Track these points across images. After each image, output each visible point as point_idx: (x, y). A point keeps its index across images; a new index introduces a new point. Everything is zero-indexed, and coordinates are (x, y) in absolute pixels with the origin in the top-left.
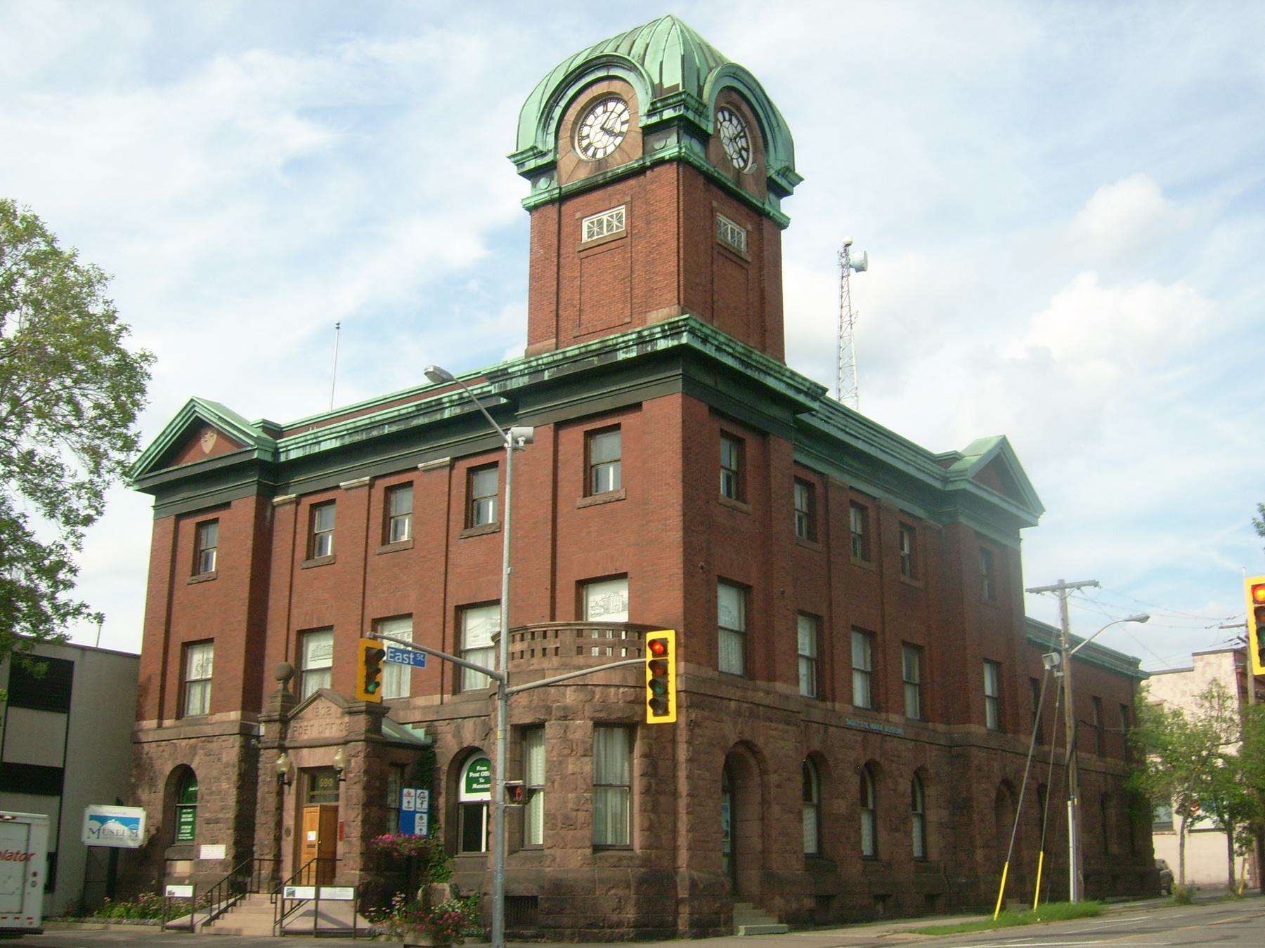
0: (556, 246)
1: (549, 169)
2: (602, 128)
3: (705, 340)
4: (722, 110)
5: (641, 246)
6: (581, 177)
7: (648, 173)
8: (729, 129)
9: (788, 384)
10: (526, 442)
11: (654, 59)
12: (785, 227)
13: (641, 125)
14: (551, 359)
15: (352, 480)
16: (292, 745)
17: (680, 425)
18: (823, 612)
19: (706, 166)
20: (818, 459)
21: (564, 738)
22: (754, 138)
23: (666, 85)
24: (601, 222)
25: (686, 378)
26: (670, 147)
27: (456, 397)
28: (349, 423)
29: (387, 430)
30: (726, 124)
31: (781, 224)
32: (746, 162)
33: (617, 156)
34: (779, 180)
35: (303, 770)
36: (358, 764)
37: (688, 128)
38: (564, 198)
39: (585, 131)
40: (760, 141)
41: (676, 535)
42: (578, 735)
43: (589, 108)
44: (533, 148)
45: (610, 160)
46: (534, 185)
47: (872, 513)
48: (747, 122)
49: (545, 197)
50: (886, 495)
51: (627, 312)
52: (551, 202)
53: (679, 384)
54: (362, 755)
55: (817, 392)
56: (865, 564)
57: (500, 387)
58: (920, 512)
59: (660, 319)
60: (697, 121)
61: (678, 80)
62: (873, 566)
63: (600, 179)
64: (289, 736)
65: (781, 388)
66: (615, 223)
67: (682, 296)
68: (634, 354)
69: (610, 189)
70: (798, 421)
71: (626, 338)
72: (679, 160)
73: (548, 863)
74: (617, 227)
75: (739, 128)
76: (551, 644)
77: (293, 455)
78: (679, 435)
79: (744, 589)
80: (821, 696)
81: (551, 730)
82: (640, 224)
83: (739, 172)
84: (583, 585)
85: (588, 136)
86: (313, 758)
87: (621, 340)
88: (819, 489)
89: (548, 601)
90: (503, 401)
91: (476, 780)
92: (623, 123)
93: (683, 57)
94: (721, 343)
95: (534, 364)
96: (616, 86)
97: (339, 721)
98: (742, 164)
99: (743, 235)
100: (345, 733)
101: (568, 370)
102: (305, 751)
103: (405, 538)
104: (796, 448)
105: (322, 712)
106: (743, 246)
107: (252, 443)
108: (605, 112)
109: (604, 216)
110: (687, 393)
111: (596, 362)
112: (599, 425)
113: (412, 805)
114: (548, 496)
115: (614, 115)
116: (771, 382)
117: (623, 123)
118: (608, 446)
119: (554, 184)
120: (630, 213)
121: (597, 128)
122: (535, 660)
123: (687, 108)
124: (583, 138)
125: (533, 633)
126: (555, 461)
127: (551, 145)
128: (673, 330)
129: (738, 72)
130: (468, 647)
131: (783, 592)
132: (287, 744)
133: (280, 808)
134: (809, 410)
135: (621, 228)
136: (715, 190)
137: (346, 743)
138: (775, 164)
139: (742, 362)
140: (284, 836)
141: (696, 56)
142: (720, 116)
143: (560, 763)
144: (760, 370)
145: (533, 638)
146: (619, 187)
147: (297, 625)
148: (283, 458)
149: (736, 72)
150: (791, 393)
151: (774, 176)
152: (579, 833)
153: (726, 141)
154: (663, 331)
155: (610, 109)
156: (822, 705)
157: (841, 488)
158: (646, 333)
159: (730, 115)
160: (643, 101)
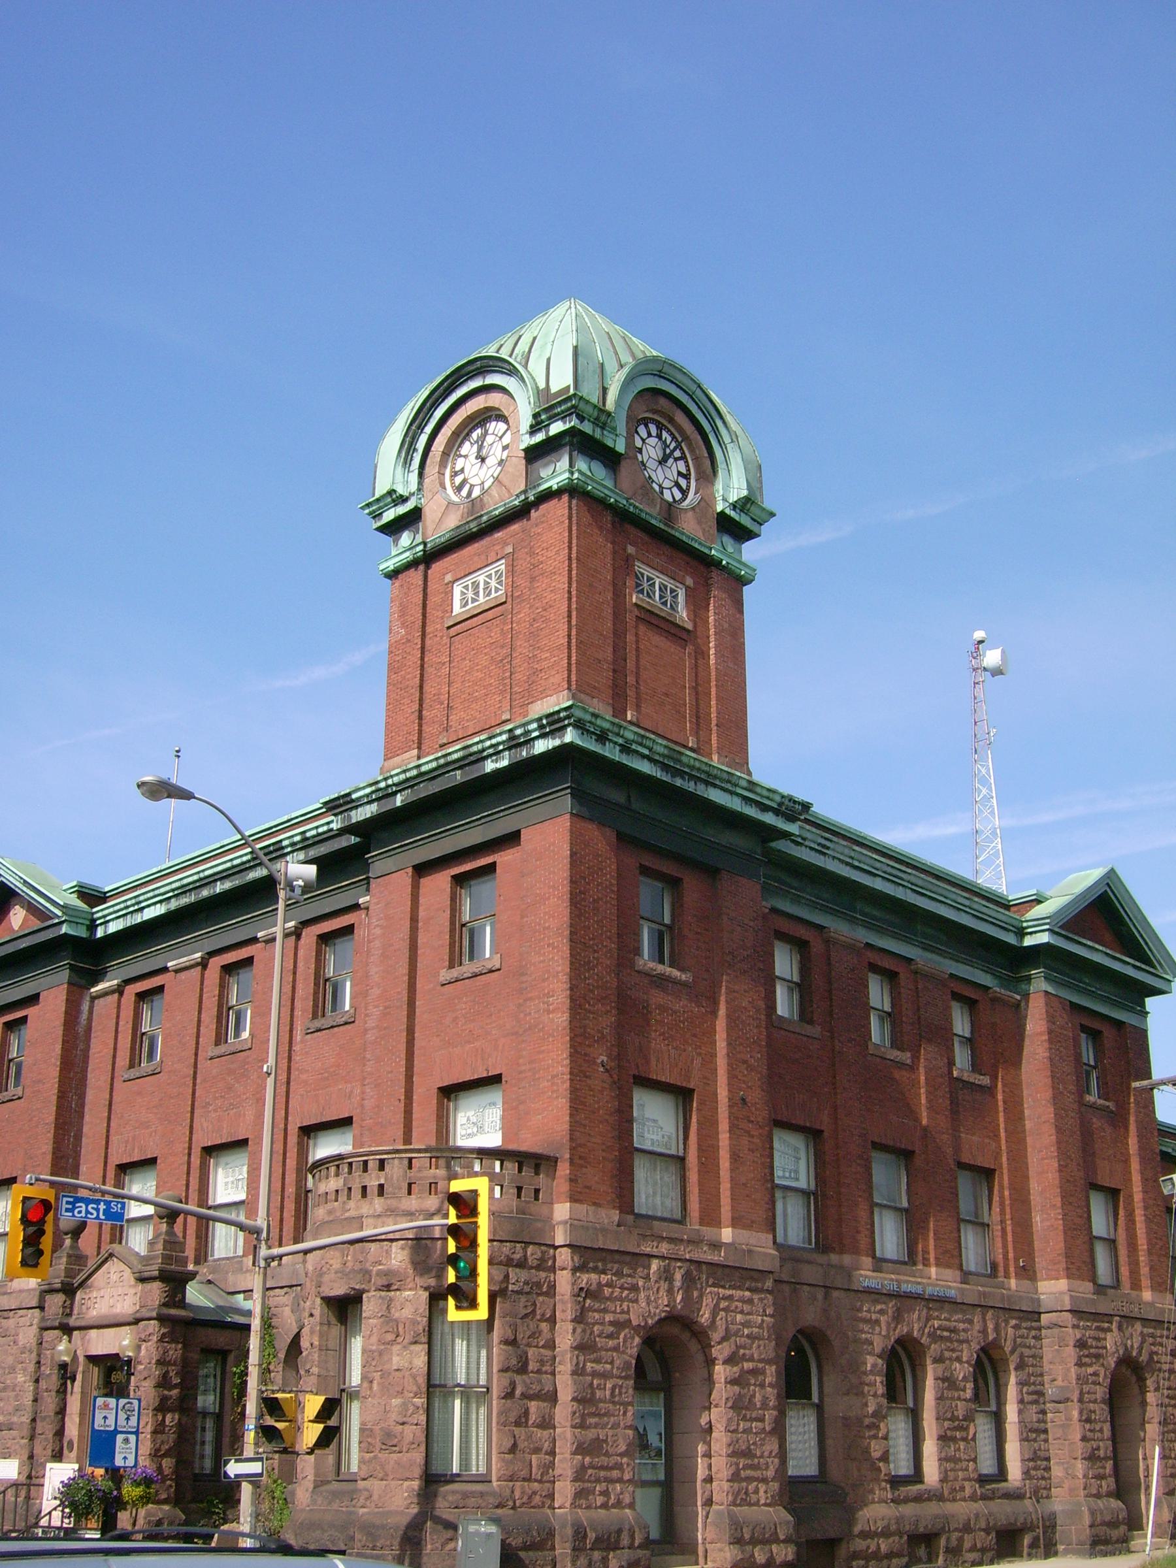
1: (413, 518)
3: (602, 738)
4: (645, 422)
5: (523, 614)
6: (452, 522)
9: (745, 798)
11: (540, 356)
12: (750, 582)
13: (523, 446)
14: (402, 777)
15: (181, 956)
16: (78, 1324)
17: (567, 861)
18: (824, 1122)
20: (814, 906)
21: (387, 1318)
22: (696, 459)
23: (554, 388)
24: (472, 588)
25: (578, 795)
26: (558, 472)
27: (298, 838)
28: (175, 882)
29: (219, 888)
32: (684, 493)
33: (494, 493)
35: (93, 1359)
36: (148, 1353)
37: (583, 444)
38: (430, 557)
39: (460, 463)
41: (562, 1019)
42: (406, 1313)
44: (391, 492)
45: (486, 498)
48: (686, 438)
50: (929, 955)
51: (506, 705)
53: (567, 801)
54: (155, 1338)
55: (796, 810)
57: (343, 820)
58: (985, 979)
60: (598, 435)
61: (568, 380)
64: (75, 1312)
65: (735, 804)
66: (493, 583)
67: (574, 678)
68: (504, 763)
70: (768, 852)
71: (494, 741)
72: (571, 490)
73: (362, 1501)
74: (497, 590)
76: (373, 1180)
77: (113, 928)
78: (567, 874)
80: (823, 1247)
81: (371, 1305)
82: (521, 581)
84: (451, 1092)
85: (462, 471)
86: (103, 1343)
87: (488, 743)
88: (817, 947)
89: (400, 1117)
90: (353, 840)
93: (576, 348)
94: (627, 741)
95: (382, 785)
96: (494, 400)
97: (132, 1291)
98: (678, 496)
102: (93, 1332)
103: (245, 1035)
104: (766, 890)
105: (114, 1277)
107: (60, 913)
109: (481, 577)
111: (459, 776)
112: (471, 869)
113: (111, 1421)
114: (403, 969)
117: (505, 448)
119: (419, 539)
120: (512, 570)
121: (472, 458)
122: (352, 1204)
123: (581, 418)
124: (455, 474)
125: (350, 1164)
126: (414, 919)
127: (413, 487)
128: (553, 724)
132: (72, 1322)
133: (62, 1412)
134: (786, 835)
135: (498, 594)
136: (633, 531)
137: (137, 1321)
139: (665, 767)
140: (65, 1451)
142: (642, 430)
143: (381, 1354)
144: (697, 780)
145: (350, 1172)
146: (498, 535)
147: (116, 1159)
148: (100, 933)
150: (751, 812)
151: (728, 511)
152: (405, 1457)
153: (652, 464)
154: (541, 727)
156: (821, 1259)
157: (851, 947)
158: (518, 732)
159: (660, 427)
160: (524, 410)
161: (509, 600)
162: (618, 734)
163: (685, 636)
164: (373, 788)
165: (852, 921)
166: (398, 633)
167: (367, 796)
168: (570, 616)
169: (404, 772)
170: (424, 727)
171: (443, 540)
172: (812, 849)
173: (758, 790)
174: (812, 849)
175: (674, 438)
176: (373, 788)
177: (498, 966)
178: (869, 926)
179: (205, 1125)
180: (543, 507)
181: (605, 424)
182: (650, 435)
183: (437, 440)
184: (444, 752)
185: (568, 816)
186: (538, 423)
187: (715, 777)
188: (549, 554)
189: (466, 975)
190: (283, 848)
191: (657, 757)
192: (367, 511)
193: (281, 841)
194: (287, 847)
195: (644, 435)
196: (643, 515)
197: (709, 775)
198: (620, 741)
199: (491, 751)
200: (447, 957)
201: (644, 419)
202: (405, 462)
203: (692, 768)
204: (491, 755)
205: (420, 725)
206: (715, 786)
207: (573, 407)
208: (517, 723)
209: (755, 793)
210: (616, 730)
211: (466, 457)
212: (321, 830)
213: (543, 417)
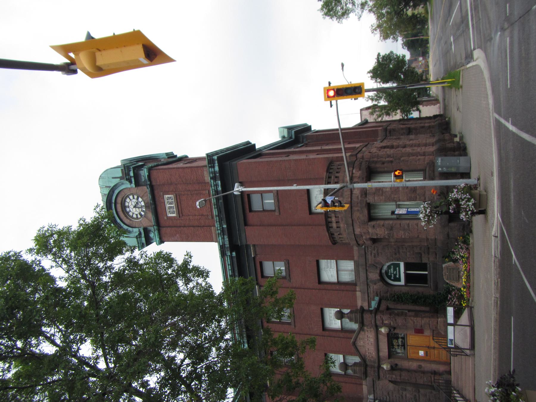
6: (150, 215)
7: (154, 183)
13: (134, 186)
14: (218, 223)
52: (159, 231)
63: (153, 206)
66: (170, 201)
68: (219, 182)
85: (137, 215)
91: (395, 275)
95: (219, 231)
96: (119, 200)
100: (372, 329)
101: (223, 216)
109: (168, 206)
124: (137, 217)
130: (340, 327)
140: (422, 369)
179: (316, 329)
180: (152, 180)
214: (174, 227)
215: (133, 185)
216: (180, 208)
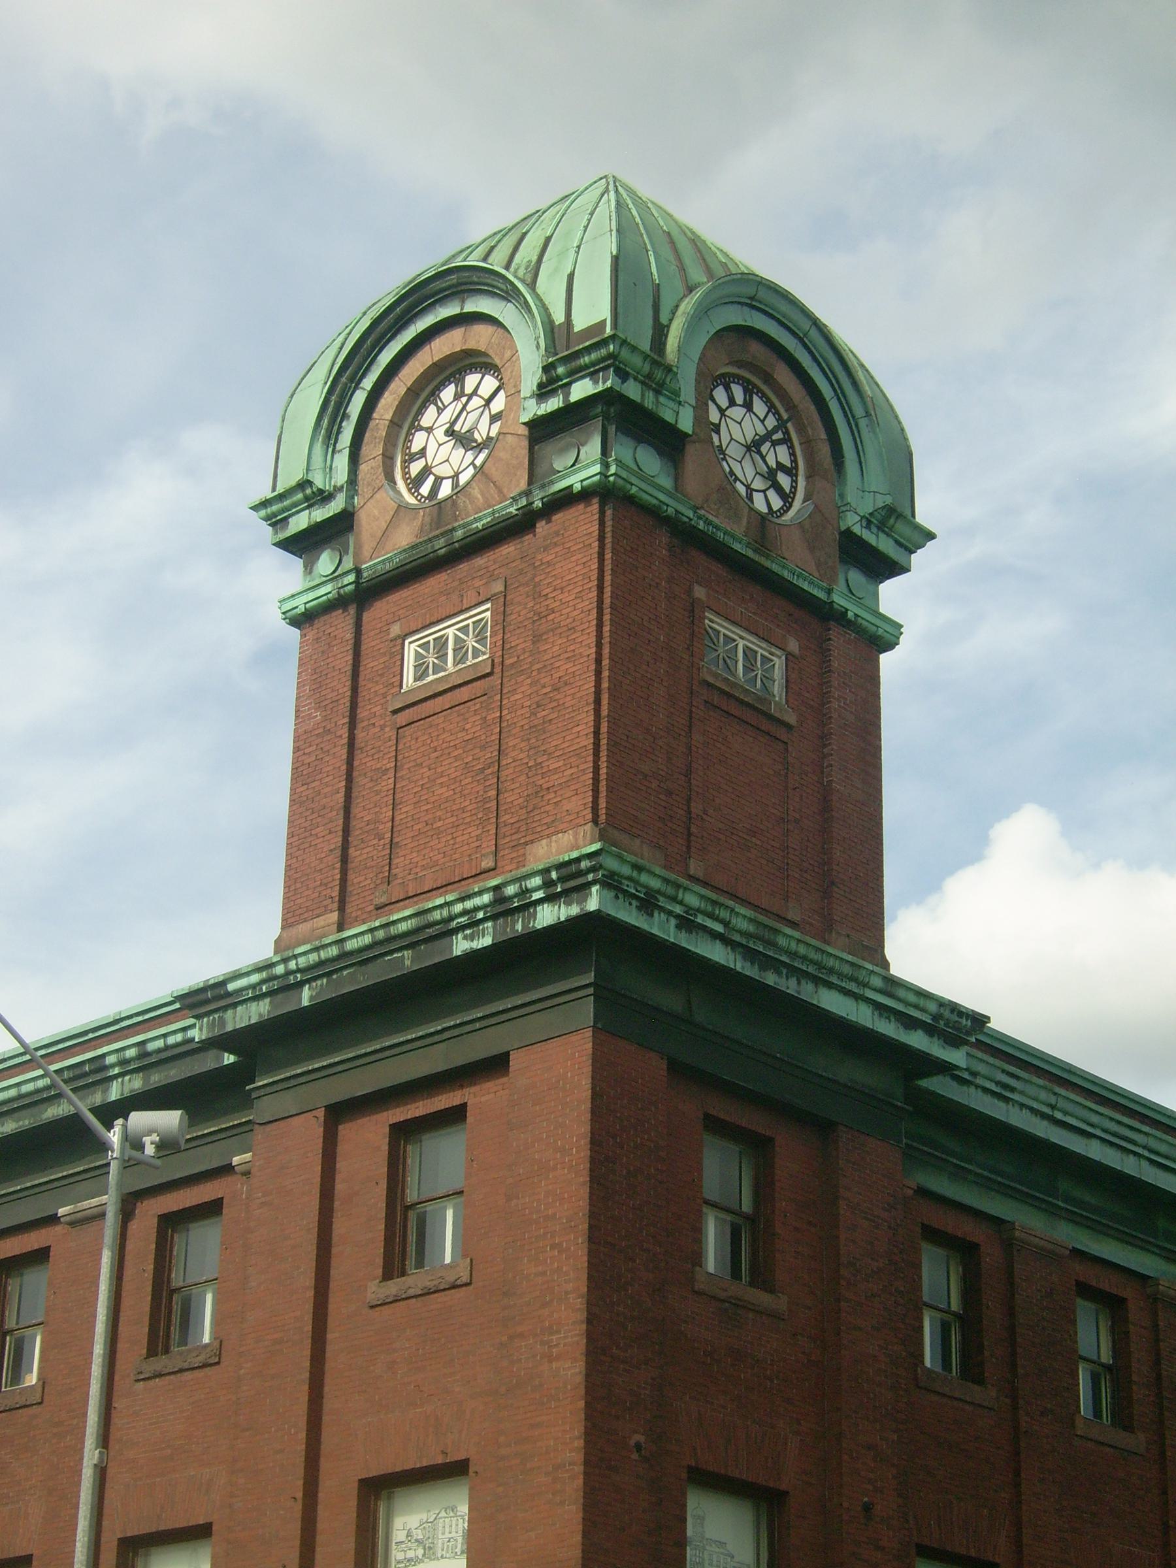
0: (346, 701)
1: (337, 530)
2: (450, 432)
3: (648, 904)
6: (405, 537)
7: (541, 527)
8: (740, 424)
9: (879, 1007)
10: (160, 1146)
11: (556, 270)
12: (890, 646)
13: (525, 417)
14: (313, 958)
17: (586, 1106)
19: (672, 506)
20: (986, 1185)
22: (807, 443)
23: (580, 323)
26: (582, 464)
27: (131, 1053)
30: (737, 412)
31: (881, 638)
32: (787, 498)
33: (476, 492)
34: (869, 537)
38: (367, 593)
40: (825, 450)
41: (571, 1371)
43: (424, 392)
44: (304, 484)
45: (461, 500)
46: (309, 568)
47: (1136, 1311)
48: (791, 407)
49: (327, 591)
53: (588, 1008)
56: (1121, 1438)
57: (211, 1026)
59: (548, 852)
60: (649, 401)
61: (603, 312)
62: (1137, 1441)
65: (862, 1015)
66: (471, 643)
67: (602, 803)
68: (487, 941)
69: (463, 568)
71: (469, 904)
72: (601, 493)
75: (771, 422)
78: (585, 1129)
79: (766, 1500)
83: (763, 523)
85: (423, 452)
87: (458, 908)
88: (991, 1256)
90: (229, 1059)
92: (494, 418)
93: (616, 260)
95: (280, 970)
96: (479, 337)
98: (777, 503)
99: (779, 663)
103: (32, 1379)
106: (778, 689)
108: (457, 397)
109: (450, 631)
110: (604, 1029)
111: (408, 960)
112: (423, 1112)
114: (306, 1279)
115: (476, 402)
116: (831, 1002)
117: (494, 418)
118: (444, 1160)
119: (348, 564)
121: (440, 433)
123: (623, 375)
124: (411, 458)
127: (341, 475)
128: (567, 880)
129: (762, 294)
131: (867, 1508)
134: (945, 1068)
135: (480, 656)
138: (860, 498)
139: (750, 955)
141: (647, 256)
142: (720, 395)
146: (479, 561)
149: (758, 294)
150: (888, 1028)
151: (857, 530)
153: (734, 451)
154: (548, 884)
155: (469, 389)
158: (511, 890)
159: (749, 390)
160: (529, 359)
161: (498, 670)
162: (674, 899)
163: (781, 733)
164: (264, 975)
165: (1053, 1212)
166: (310, 717)
167: (253, 987)
168: (598, 702)
169: (317, 949)
170: (351, 876)
171: (388, 567)
172: (986, 1090)
173: (901, 993)
174: (986, 1090)
175: (771, 408)
176: (264, 975)
177: (465, 1278)
178: (1074, 1219)
180: (557, 517)
181: (662, 385)
182: (732, 403)
183: (382, 402)
184: (384, 920)
185: (588, 1033)
186: (552, 380)
187: (831, 971)
188: (565, 597)
189: (411, 1292)
190: (106, 1068)
191: (737, 938)
192: (263, 513)
193: (103, 1056)
194: (113, 1066)
195: (724, 403)
196: (720, 535)
197: (820, 966)
198: (678, 909)
199: (463, 920)
200: (379, 1261)
201: (723, 375)
202: (328, 436)
203: (794, 955)
204: (463, 928)
205: (344, 872)
206: (830, 985)
207: (611, 356)
208: (509, 876)
209: (899, 1000)
210: (670, 891)
211: (429, 430)
212: (171, 1040)
213: (561, 370)
214: (355, 689)
215: (533, 409)
216: (430, 707)
